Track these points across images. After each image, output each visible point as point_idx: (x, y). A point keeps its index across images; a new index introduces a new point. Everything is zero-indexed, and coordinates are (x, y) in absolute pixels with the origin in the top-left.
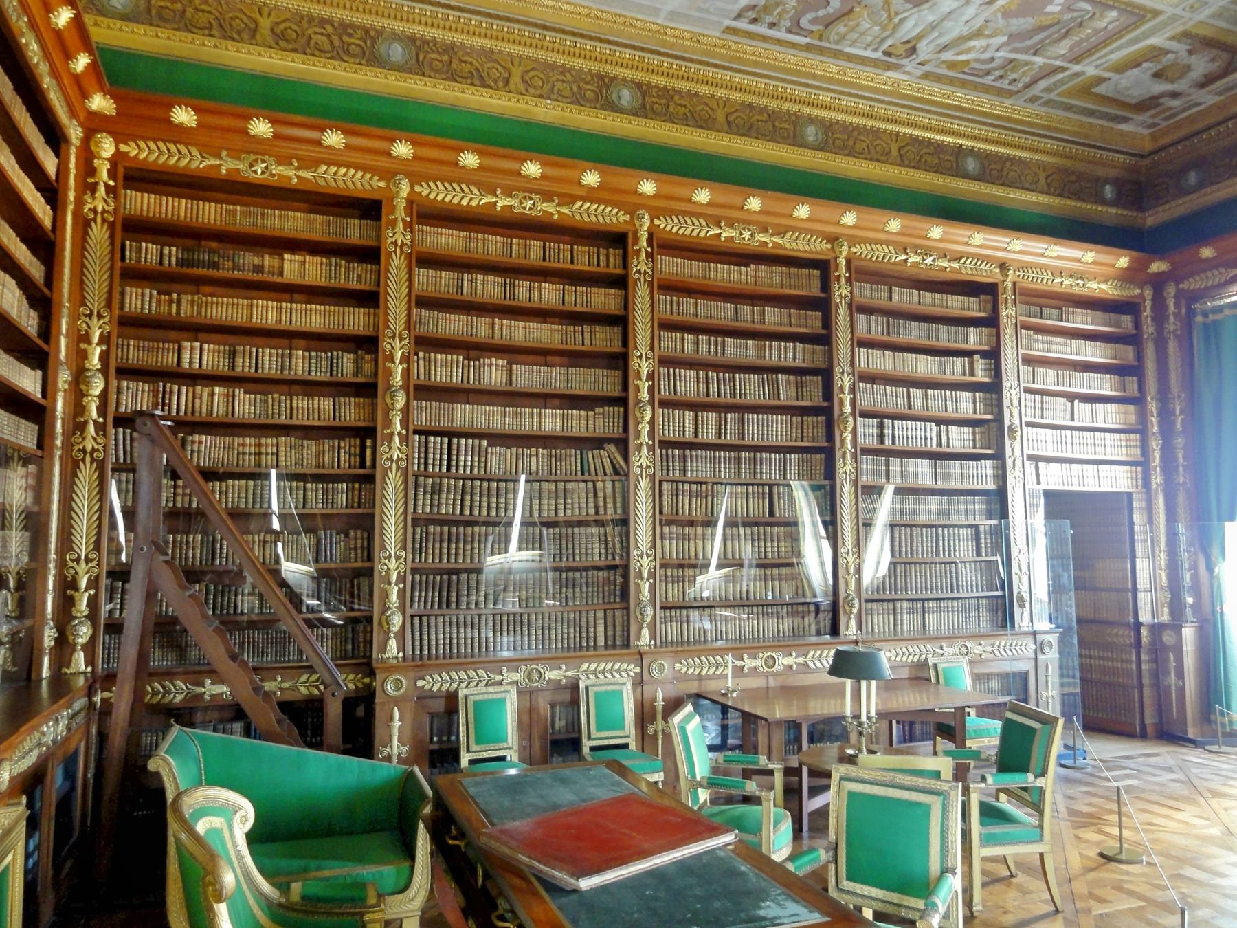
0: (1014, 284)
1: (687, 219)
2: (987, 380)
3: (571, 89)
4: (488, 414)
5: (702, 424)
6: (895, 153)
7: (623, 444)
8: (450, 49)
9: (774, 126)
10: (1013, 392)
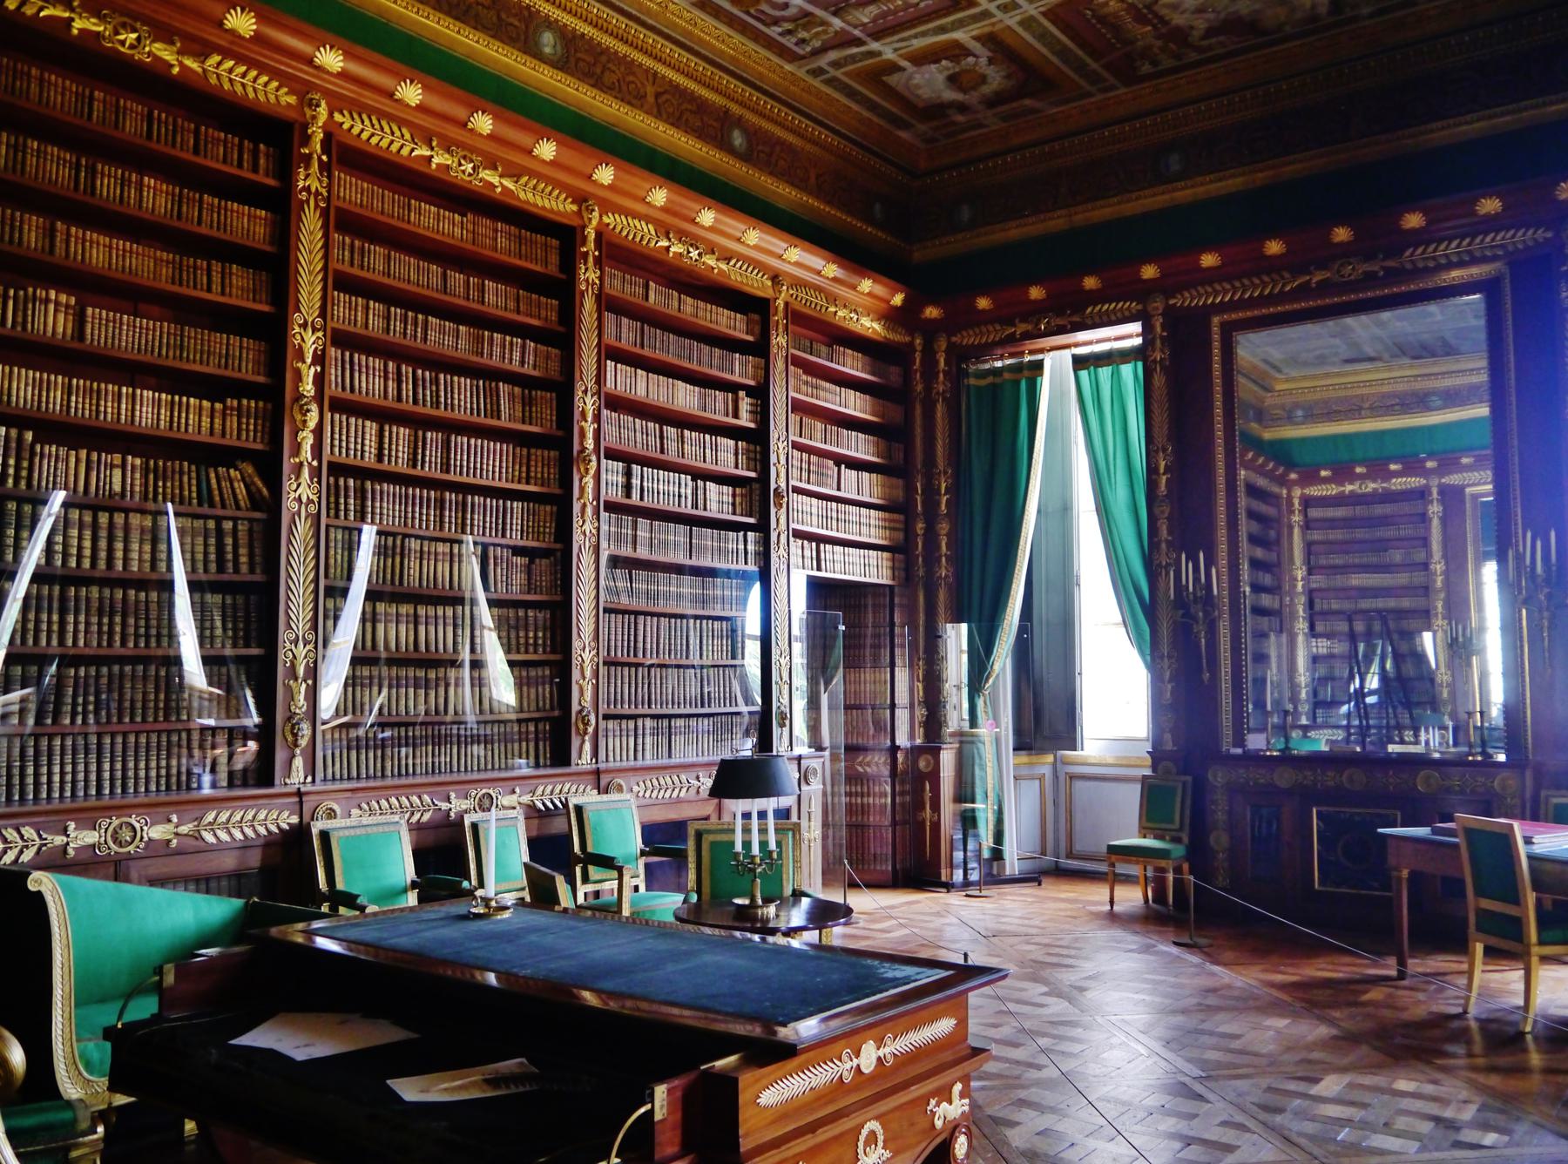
0: (787, 304)
1: (384, 123)
2: (752, 425)
4: (39, 385)
5: (390, 444)
6: (651, 99)
7: (270, 467)
9: (499, 17)
10: (780, 444)
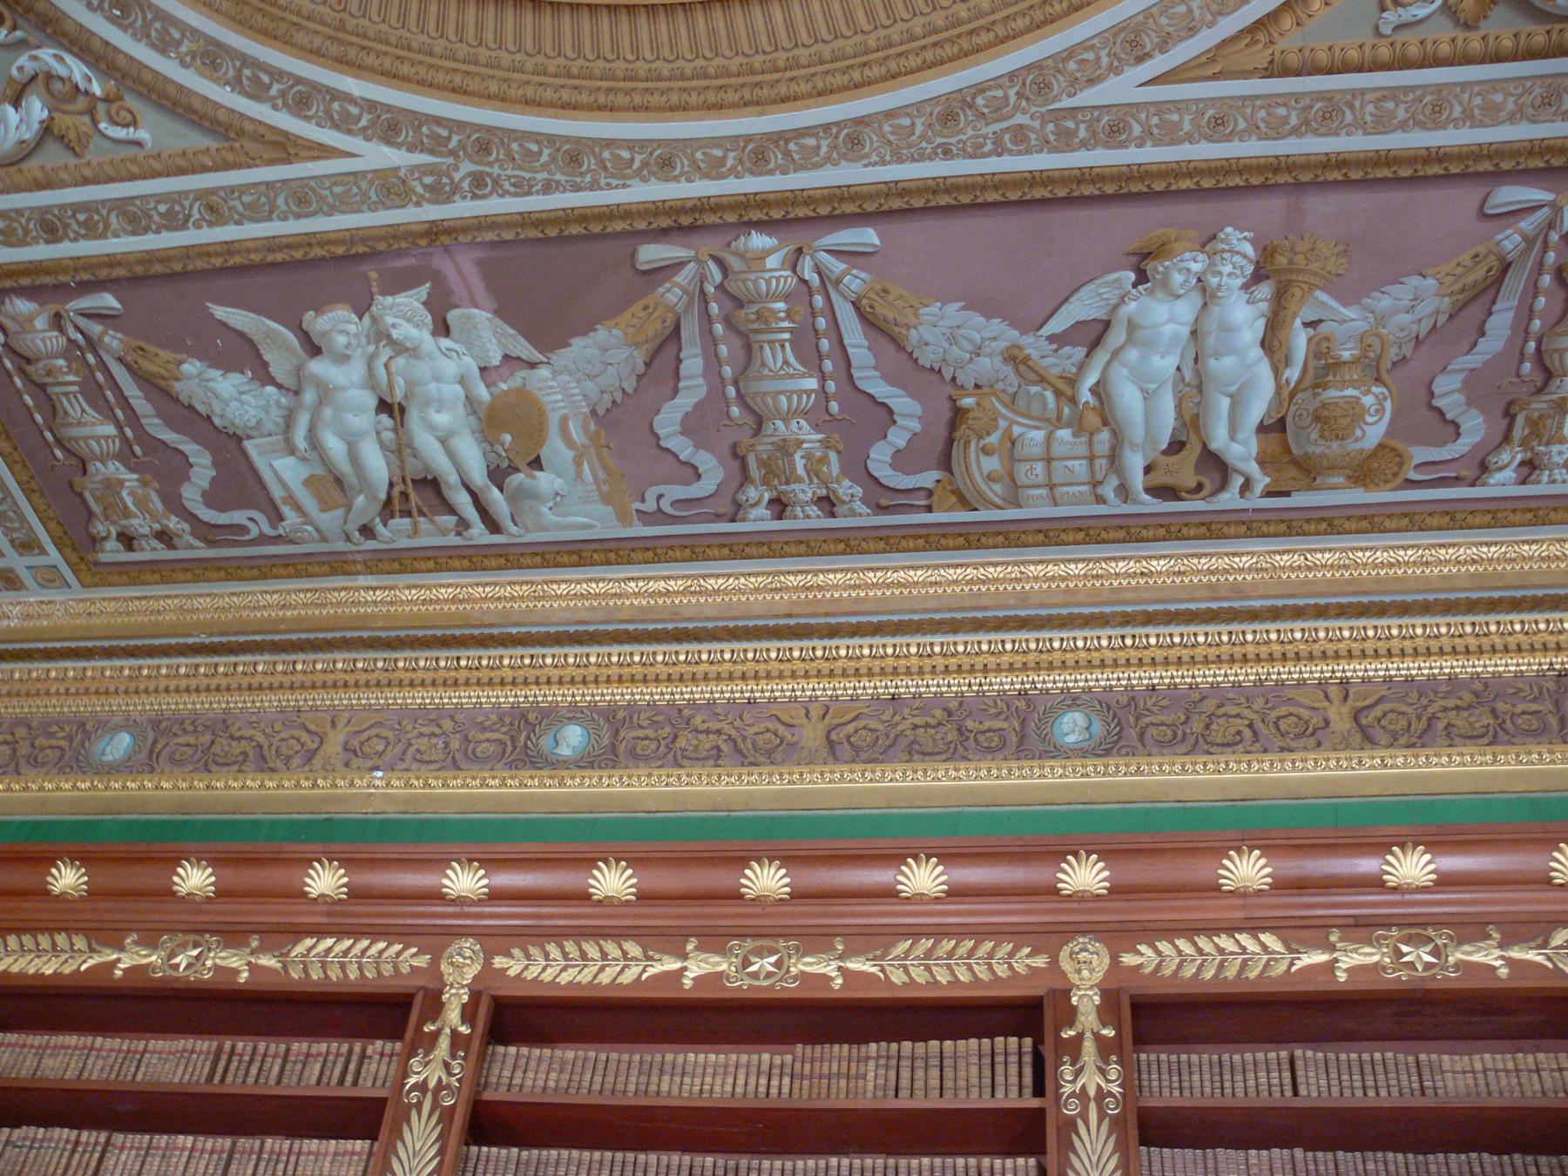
3: (447, 745)
8: (222, 725)
